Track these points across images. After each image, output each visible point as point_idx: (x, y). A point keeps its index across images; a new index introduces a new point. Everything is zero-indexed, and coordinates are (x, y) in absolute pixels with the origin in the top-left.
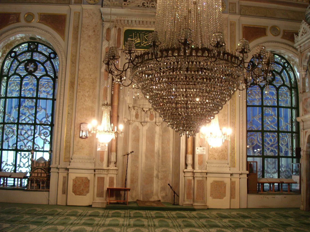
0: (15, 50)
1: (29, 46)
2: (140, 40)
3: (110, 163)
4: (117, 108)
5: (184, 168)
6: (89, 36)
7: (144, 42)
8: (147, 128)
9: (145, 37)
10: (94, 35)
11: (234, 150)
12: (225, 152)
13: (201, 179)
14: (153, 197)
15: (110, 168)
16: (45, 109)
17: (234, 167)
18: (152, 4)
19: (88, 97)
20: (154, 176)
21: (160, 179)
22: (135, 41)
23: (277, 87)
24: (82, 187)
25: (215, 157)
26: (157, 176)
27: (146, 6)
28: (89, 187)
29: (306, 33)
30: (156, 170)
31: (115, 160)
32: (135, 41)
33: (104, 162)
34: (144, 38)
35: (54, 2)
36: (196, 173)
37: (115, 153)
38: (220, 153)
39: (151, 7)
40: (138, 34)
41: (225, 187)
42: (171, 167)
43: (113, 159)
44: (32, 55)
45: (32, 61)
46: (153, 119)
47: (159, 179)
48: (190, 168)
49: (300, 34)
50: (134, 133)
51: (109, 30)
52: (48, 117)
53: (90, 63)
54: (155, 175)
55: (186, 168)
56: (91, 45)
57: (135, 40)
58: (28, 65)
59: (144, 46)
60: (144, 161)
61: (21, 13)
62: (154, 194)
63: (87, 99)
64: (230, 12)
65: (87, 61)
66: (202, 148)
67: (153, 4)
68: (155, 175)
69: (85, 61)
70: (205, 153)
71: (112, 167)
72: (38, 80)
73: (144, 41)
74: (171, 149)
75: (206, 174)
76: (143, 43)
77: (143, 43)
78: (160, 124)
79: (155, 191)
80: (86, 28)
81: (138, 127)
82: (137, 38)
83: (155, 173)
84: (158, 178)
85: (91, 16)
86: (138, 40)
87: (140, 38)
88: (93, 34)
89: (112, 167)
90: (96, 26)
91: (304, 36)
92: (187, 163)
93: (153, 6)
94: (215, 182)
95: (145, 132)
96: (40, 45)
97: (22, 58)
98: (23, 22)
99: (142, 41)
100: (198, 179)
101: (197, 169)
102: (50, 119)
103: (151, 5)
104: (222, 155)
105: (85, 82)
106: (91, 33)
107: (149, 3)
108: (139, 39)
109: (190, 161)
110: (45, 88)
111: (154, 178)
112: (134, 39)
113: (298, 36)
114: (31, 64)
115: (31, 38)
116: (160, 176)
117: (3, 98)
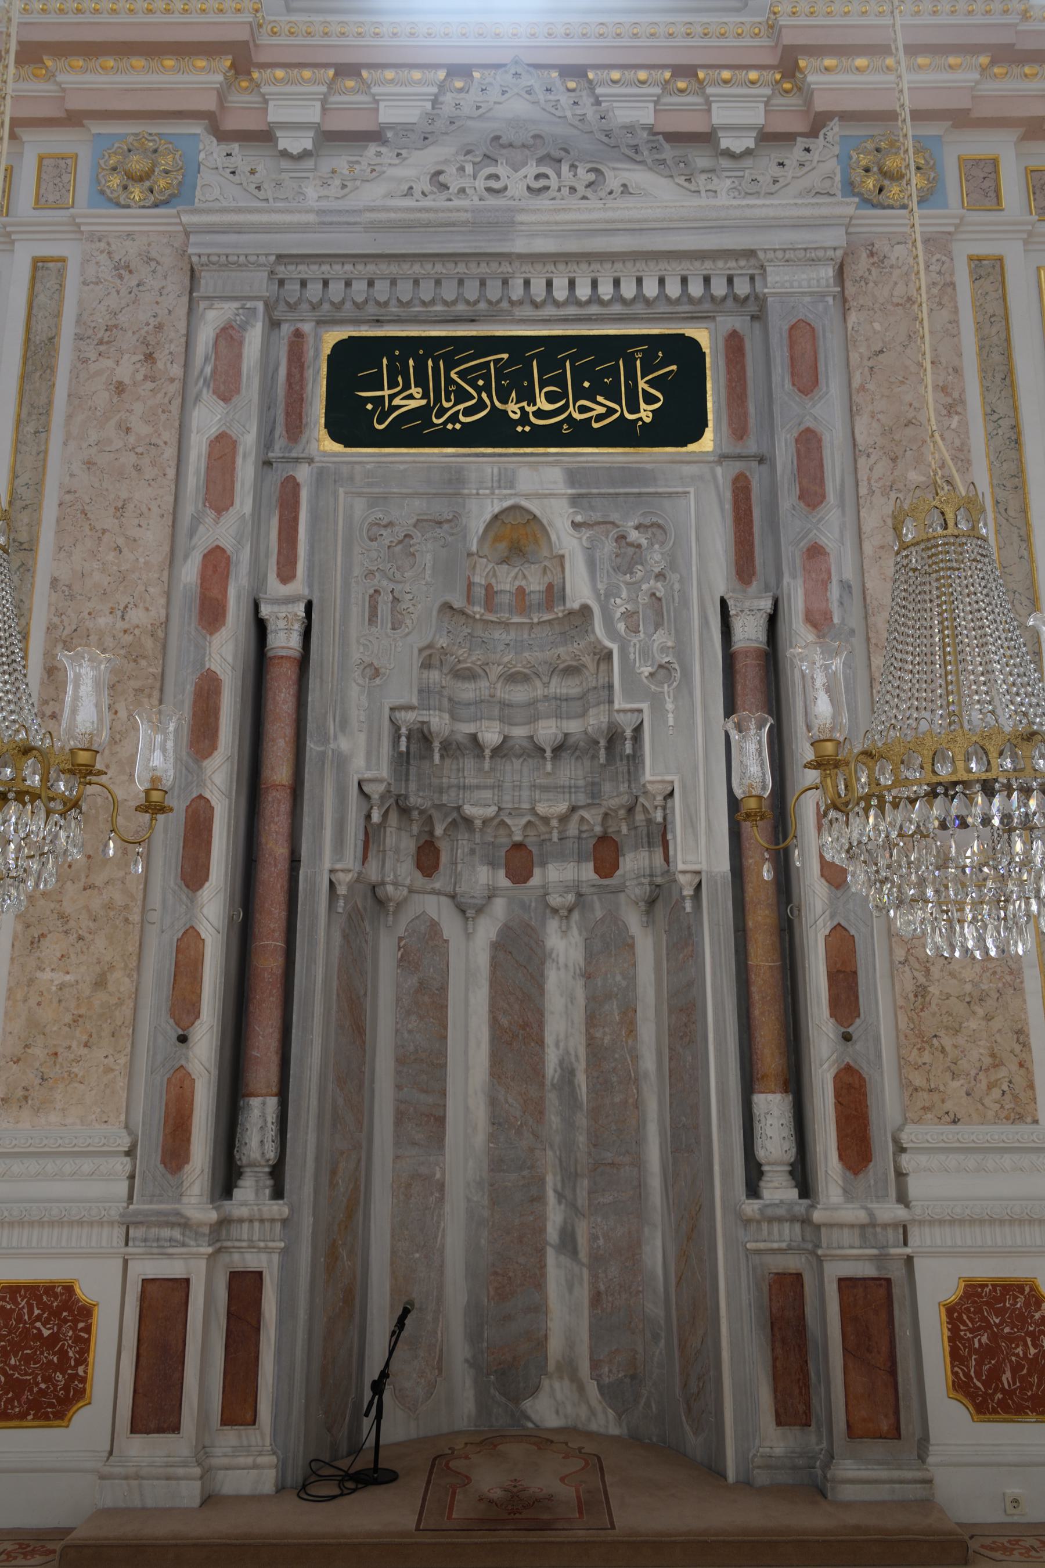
2: (425, 395)
3: (240, 1175)
4: (285, 807)
6: (120, 388)
7: (446, 405)
8: (493, 935)
10: (146, 377)
12: (1014, 1067)
13: (868, 1270)
14: (546, 1383)
18: (490, 177)
20: (547, 1243)
22: (397, 402)
25: (948, 1106)
26: (568, 1242)
27: (454, 188)
30: (560, 1196)
31: (271, 1154)
32: (397, 402)
33: (187, 1168)
34: (449, 381)
36: (831, 1226)
37: (272, 1102)
38: (982, 1076)
39: (485, 194)
40: (411, 362)
43: (257, 1141)
46: (530, 875)
47: (583, 1265)
48: (778, 1189)
50: (406, 961)
51: (229, 336)
53: (121, 541)
54: (552, 1233)
55: (753, 1191)
56: (132, 439)
57: (392, 397)
59: (450, 426)
62: (551, 1366)
65: (104, 531)
67: (496, 177)
68: (552, 1233)
69: (92, 528)
73: (448, 400)
74: (649, 1062)
78: (571, 898)
79: (555, 1346)
80: (101, 342)
81: (434, 927)
82: (407, 386)
83: (555, 1216)
84: (574, 1253)
85: (130, 272)
86: (411, 397)
88: (139, 377)
89: (250, 1194)
90: (159, 327)
92: (761, 1154)
93: (495, 185)
94: (973, 1290)
95: (482, 959)
99: (437, 399)
103: (481, 184)
104: (996, 1093)
106: (127, 369)
107: (469, 169)
109: (775, 1142)
112: (386, 393)
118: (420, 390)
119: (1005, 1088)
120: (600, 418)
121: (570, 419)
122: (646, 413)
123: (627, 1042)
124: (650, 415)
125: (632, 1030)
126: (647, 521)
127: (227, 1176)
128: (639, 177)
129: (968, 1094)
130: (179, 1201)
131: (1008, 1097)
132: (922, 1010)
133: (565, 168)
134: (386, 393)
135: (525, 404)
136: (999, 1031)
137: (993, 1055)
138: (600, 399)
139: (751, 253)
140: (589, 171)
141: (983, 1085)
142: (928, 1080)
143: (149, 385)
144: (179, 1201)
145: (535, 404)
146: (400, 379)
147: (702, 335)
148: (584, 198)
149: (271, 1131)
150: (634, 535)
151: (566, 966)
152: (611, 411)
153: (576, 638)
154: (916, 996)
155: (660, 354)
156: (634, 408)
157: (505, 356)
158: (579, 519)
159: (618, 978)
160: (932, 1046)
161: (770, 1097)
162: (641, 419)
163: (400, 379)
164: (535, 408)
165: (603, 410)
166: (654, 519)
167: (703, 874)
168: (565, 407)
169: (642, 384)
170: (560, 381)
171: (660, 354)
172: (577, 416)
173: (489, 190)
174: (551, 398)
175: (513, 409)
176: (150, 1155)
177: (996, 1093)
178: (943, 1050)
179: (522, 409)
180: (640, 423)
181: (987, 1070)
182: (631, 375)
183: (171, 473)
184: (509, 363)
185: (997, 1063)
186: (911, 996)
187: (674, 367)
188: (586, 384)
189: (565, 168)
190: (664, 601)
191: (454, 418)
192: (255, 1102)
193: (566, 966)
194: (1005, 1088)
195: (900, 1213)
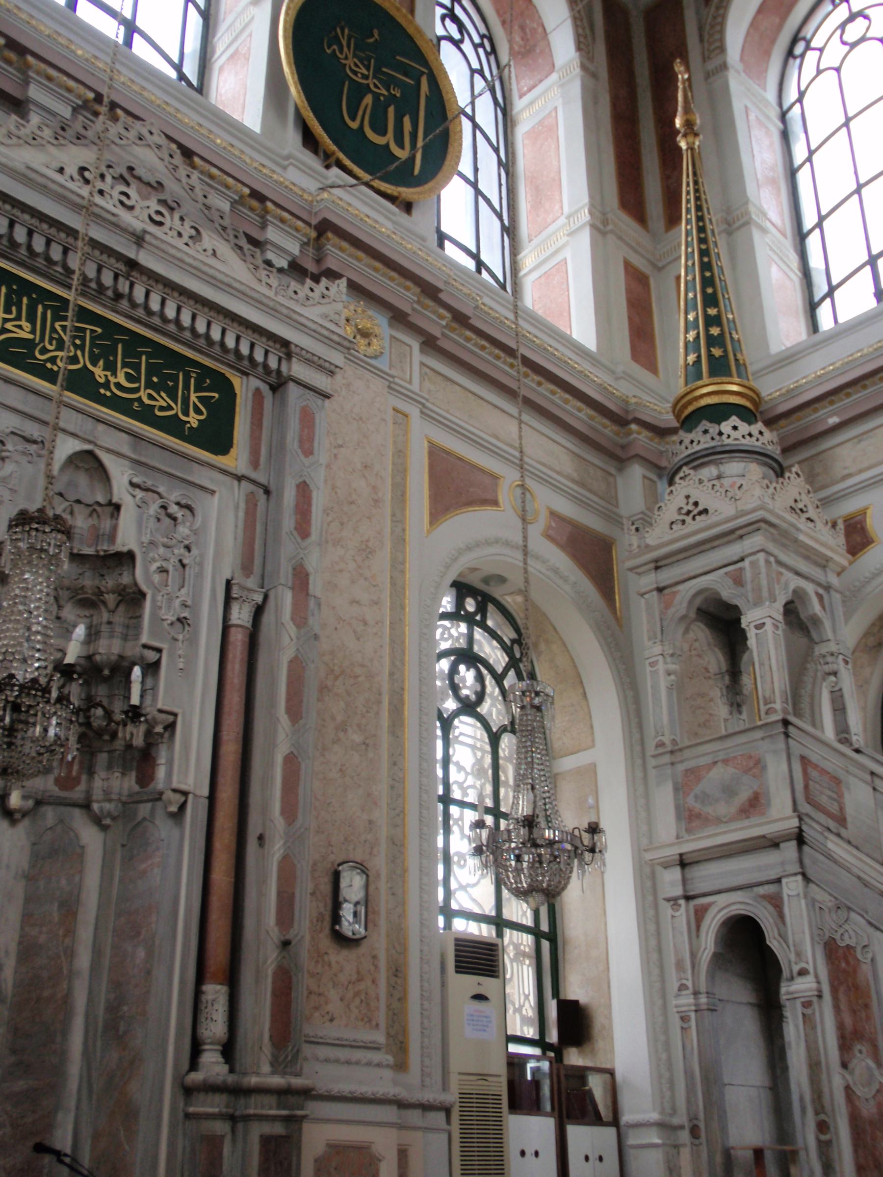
2: (33, 332)
5: (186, 1065)
9: (57, 325)
11: (399, 981)
12: (369, 983)
13: (278, 1129)
22: (9, 326)
34: (53, 330)
39: (118, 204)
55: (194, 1065)
59: (49, 365)
73: (51, 344)
74: (84, 960)
76: (44, 351)
77: (44, 351)
86: (20, 327)
87: (31, 319)
99: (42, 339)
100: (268, 1129)
104: (357, 1001)
108: (27, 326)
109: (215, 1027)
118: (29, 325)
119: (363, 998)
120: (162, 409)
121: (139, 399)
122: (193, 420)
123: (63, 942)
124: (197, 422)
125: (71, 932)
126: (183, 502)
128: (225, 249)
129: (342, 1000)
131: (364, 1005)
132: (320, 932)
133: (176, 216)
135: (109, 373)
136: (363, 955)
137: (358, 972)
138: (163, 394)
140: (193, 227)
142: (319, 986)
145: (116, 377)
146: (14, 309)
147: (237, 381)
148: (187, 244)
150: (173, 509)
151: (8, 866)
152: (169, 408)
153: (106, 577)
154: (317, 921)
155: (208, 381)
156: (186, 413)
157: (99, 330)
158: (135, 480)
159: (64, 882)
160: (323, 960)
161: (219, 987)
162: (189, 422)
163: (14, 309)
164: (116, 381)
165: (165, 404)
166: (189, 503)
167: (191, 797)
168: (137, 390)
169: (193, 397)
170: (137, 367)
171: (208, 381)
172: (147, 401)
173: (121, 202)
174: (129, 378)
175: (99, 372)
177: (357, 1001)
178: (330, 965)
179: (106, 376)
180: (188, 425)
181: (354, 983)
182: (187, 387)
184: (100, 337)
185: (360, 979)
186: (315, 920)
187: (216, 395)
188: (155, 379)
189: (176, 216)
190: (187, 568)
191: (53, 360)
193: (8, 866)
194: (363, 998)
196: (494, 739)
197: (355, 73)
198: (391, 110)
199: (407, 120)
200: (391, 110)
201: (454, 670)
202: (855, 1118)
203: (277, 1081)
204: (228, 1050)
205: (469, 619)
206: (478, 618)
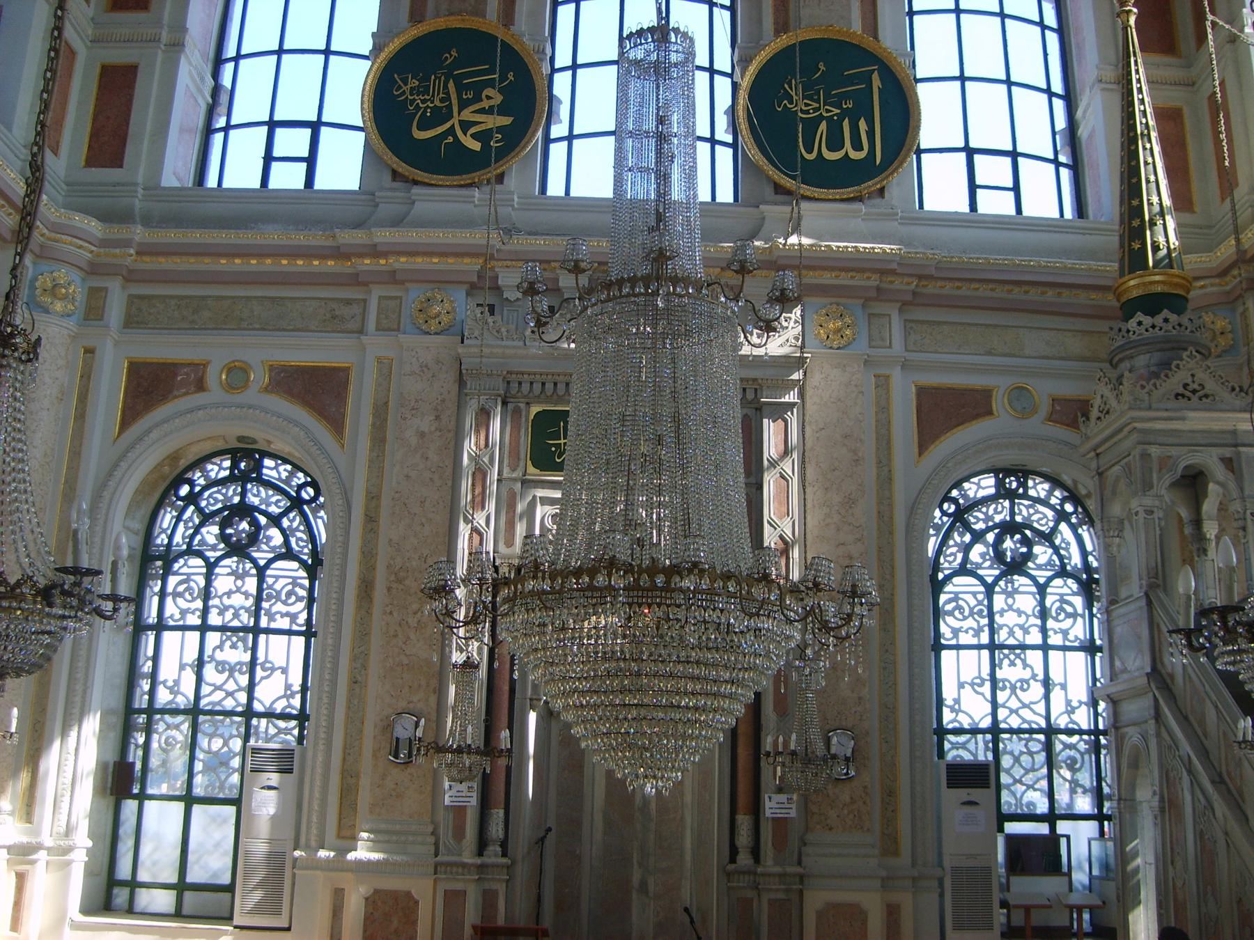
0: (189, 475)
1: (234, 465)
6: (422, 435)
13: (781, 896)
15: (486, 860)
16: (285, 671)
17: (896, 853)
19: (416, 629)
21: (651, 894)
23: (1042, 581)
24: (396, 923)
28: (415, 923)
29: (1108, 412)
30: (640, 865)
35: (313, 328)
41: (864, 922)
42: (688, 857)
43: (496, 829)
44: (243, 494)
45: (244, 510)
48: (744, 859)
49: (1094, 413)
52: (292, 695)
53: (424, 520)
55: (733, 859)
58: (231, 526)
60: (598, 836)
61: (208, 362)
63: (412, 636)
64: (874, 343)
66: (783, 797)
70: (793, 813)
71: (493, 855)
72: (261, 573)
75: (797, 880)
84: (647, 893)
88: (433, 429)
89: (493, 855)
90: (443, 401)
91: (1105, 422)
96: (268, 462)
97: (213, 500)
98: (215, 392)
100: (773, 896)
101: (769, 863)
102: (296, 701)
104: (851, 816)
105: (407, 582)
110: (285, 603)
111: (634, 896)
112: (562, 441)
113: (1088, 419)
114: (241, 520)
115: (241, 439)
116: (651, 887)
117: (151, 627)
127: (482, 845)
130: (460, 855)
134: (562, 441)
139: (755, 380)
141: (846, 812)
143: (438, 433)
144: (460, 855)
149: (501, 826)
176: (446, 836)
177: (851, 816)
183: (450, 484)
192: (494, 811)
195: (799, 870)
196: (1042, 590)
197: (807, 112)
198: (846, 123)
199: (863, 125)
200: (846, 123)
201: (999, 540)
202: (1176, 900)
203: (777, 869)
204: (756, 852)
205: (1011, 495)
206: (1021, 491)
